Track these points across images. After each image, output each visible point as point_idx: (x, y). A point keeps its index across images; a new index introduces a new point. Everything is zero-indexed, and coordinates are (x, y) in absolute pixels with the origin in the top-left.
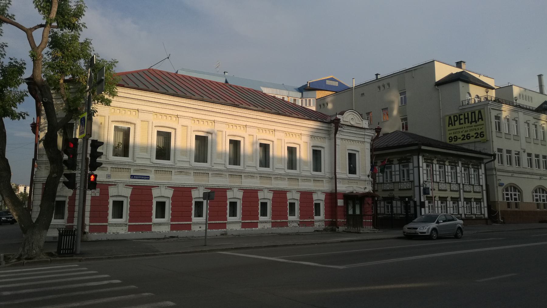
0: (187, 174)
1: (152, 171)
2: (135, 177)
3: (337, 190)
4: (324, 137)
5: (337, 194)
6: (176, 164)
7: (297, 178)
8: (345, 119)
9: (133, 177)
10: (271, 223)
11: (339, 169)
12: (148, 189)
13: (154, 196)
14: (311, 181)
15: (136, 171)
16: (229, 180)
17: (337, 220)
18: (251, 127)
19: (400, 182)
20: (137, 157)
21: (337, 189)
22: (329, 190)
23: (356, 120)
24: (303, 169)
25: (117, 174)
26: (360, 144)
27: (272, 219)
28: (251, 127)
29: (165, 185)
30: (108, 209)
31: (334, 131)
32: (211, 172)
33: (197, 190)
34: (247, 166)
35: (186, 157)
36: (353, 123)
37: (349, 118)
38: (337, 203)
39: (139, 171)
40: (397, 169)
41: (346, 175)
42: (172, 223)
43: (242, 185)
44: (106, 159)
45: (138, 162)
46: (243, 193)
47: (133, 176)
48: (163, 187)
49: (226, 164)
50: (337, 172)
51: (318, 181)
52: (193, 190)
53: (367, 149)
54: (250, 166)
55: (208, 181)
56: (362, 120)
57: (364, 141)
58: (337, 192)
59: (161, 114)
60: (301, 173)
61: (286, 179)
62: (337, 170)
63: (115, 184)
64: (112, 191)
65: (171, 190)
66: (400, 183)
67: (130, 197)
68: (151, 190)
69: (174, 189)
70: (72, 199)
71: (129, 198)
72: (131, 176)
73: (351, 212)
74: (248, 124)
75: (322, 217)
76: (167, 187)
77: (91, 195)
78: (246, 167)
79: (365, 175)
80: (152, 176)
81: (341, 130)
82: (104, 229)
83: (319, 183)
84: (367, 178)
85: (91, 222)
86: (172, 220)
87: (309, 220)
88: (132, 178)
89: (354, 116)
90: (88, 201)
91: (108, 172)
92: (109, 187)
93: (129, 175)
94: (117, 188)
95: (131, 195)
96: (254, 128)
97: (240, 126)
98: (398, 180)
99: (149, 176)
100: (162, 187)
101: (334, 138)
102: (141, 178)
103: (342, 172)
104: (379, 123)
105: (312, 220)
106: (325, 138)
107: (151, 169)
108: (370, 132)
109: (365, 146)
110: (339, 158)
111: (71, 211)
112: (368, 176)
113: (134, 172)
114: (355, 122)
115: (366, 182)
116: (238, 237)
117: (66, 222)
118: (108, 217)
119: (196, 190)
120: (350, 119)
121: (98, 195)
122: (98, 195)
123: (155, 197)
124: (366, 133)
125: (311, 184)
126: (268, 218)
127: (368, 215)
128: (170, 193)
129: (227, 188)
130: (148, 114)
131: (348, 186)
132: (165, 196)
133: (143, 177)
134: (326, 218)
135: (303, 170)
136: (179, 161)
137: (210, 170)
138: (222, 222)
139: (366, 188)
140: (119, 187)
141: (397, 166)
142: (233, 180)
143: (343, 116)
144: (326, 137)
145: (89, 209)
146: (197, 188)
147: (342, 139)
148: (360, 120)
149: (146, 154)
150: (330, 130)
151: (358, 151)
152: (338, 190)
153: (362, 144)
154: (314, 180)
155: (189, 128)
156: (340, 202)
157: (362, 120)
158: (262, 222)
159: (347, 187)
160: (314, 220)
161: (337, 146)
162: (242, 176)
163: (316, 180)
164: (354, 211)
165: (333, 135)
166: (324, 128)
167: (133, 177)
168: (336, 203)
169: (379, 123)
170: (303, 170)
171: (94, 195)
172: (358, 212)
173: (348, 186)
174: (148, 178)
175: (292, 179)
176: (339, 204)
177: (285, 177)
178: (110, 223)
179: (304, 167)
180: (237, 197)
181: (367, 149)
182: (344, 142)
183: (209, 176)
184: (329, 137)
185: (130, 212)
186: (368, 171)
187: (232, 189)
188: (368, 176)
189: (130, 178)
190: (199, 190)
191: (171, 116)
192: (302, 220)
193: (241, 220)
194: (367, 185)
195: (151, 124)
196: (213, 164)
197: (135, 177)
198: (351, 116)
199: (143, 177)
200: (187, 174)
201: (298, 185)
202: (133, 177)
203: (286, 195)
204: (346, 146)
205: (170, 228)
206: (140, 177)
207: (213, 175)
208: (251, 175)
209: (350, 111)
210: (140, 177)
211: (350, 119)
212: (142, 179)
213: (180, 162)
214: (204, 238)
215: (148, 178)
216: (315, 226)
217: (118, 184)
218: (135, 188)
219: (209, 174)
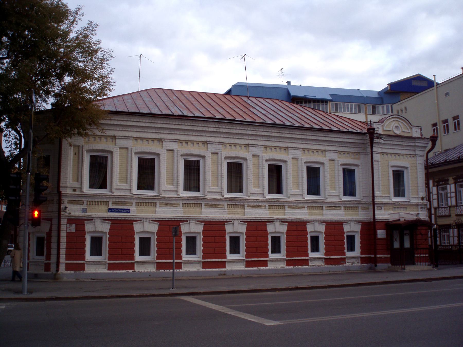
0: (174, 205)
2: (113, 210)
3: (376, 219)
4: (359, 152)
5: (376, 223)
6: (161, 194)
7: (321, 205)
8: (386, 127)
9: (111, 210)
10: (285, 261)
11: (379, 192)
12: (130, 223)
13: (135, 231)
14: (341, 208)
15: (113, 203)
16: (228, 210)
17: (375, 256)
18: (255, 146)
19: (457, 206)
20: (115, 188)
21: (376, 217)
22: (365, 219)
23: (401, 128)
24: (329, 194)
25: (94, 208)
26: (410, 158)
27: (287, 257)
28: (254, 145)
29: (149, 219)
30: (84, 246)
31: (369, 144)
32: (205, 203)
33: (188, 223)
34: (251, 193)
35: (172, 186)
36: (397, 132)
37: (392, 126)
38: (377, 234)
39: (119, 203)
40: (453, 189)
41: (390, 198)
42: (158, 261)
43: (245, 216)
44: (81, 192)
45: (116, 193)
46: (246, 226)
47: (112, 209)
48: (146, 221)
49: (223, 191)
50: (375, 195)
51: (350, 208)
52: (183, 224)
53: (421, 164)
54: (255, 194)
55: (201, 213)
56: (412, 127)
57: (415, 154)
58: (376, 221)
59: (142, 139)
60: (327, 199)
61: (306, 207)
62: (376, 193)
63: (90, 219)
64: (89, 227)
65: (156, 224)
66: (456, 207)
67: (109, 232)
68: (133, 224)
69: (159, 223)
70: (49, 234)
71: (107, 233)
72: (109, 209)
73: (396, 245)
74: (251, 142)
75: (357, 252)
76: (151, 220)
77: (66, 230)
78: (249, 194)
79: (418, 198)
80: (133, 208)
81: (380, 142)
82: (81, 267)
83: (352, 211)
84: (421, 201)
85: (67, 259)
86: (158, 258)
87: (339, 257)
89: (400, 123)
90: (64, 237)
91: (84, 206)
92: (85, 222)
93: (107, 208)
95: (110, 230)
96: (260, 146)
97: (240, 145)
98: (454, 203)
99: (129, 209)
100: (144, 221)
101: (370, 153)
102: (120, 212)
103: (384, 196)
105: (343, 257)
106: (359, 153)
107: (132, 201)
108: (423, 142)
109: (416, 160)
110: (379, 177)
111: (49, 248)
112: (423, 199)
114: (401, 130)
115: (419, 207)
116: (240, 277)
117: (45, 260)
118: (85, 254)
119: (186, 224)
120: (393, 127)
121: (73, 230)
122: (73, 230)
123: (137, 233)
124: (417, 144)
125: (341, 212)
126: (282, 255)
127: (421, 249)
128: (154, 228)
129: (226, 220)
130: (127, 140)
131: (392, 212)
132: (149, 231)
133: (122, 211)
134: (362, 253)
135: (328, 196)
136: (165, 191)
137: (202, 199)
138: (220, 260)
139: (418, 214)
140: (96, 222)
141: (453, 186)
142: (233, 211)
143: (382, 124)
144: (361, 151)
145: (65, 246)
146: (187, 221)
147: (383, 153)
148: (408, 128)
149: (125, 184)
150: (365, 142)
151: (406, 168)
152: (378, 219)
153: (413, 158)
154: (345, 207)
155: (176, 152)
156: (381, 234)
157: (412, 127)
158: (273, 260)
159: (392, 214)
160: (345, 257)
161: (374, 163)
162: (245, 205)
163: (348, 207)
164: (402, 243)
165: (369, 150)
166: (357, 141)
167: (111, 210)
168: (376, 234)
170: (328, 196)
171: (70, 231)
172: (407, 245)
173: (392, 212)
174: (128, 211)
175: (312, 206)
176: (379, 236)
177: (304, 205)
178: (87, 260)
179: (330, 191)
180: (238, 231)
181: (419, 164)
182: (386, 156)
183: (201, 207)
184: (365, 152)
185: (109, 248)
186: (422, 193)
187: (231, 221)
188: (423, 199)
191: (153, 140)
192: (328, 257)
193: (245, 258)
194: (420, 209)
195: (129, 151)
196: (206, 193)
197: (113, 210)
198: (394, 124)
199: (122, 211)
200: (175, 206)
201: (322, 214)
203: (306, 227)
204: (389, 162)
205: (156, 267)
206: (120, 210)
207: (207, 205)
208: (257, 204)
209: (393, 116)
211: (394, 127)
212: (122, 212)
213: (166, 192)
214: (172, 278)
215: (128, 211)
216: (348, 264)
217: (95, 218)
218: (115, 223)
219: (202, 205)
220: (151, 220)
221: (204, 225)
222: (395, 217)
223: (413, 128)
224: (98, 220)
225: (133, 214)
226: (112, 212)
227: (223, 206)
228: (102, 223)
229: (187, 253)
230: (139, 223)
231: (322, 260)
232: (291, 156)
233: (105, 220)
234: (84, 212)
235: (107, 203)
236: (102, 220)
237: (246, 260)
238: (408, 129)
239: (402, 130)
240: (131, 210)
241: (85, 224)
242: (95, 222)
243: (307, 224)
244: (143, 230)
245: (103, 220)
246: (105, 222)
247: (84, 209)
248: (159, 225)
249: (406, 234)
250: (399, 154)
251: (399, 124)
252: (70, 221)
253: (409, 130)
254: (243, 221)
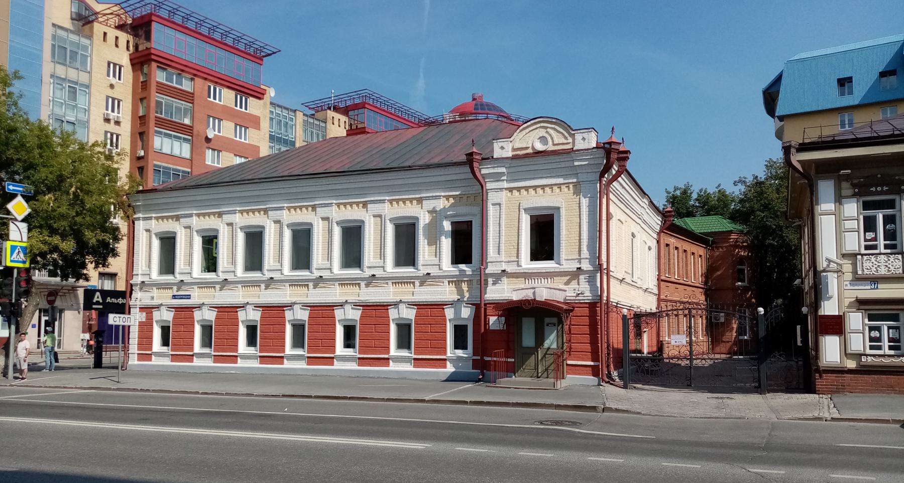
9: (174, 297)
12: (190, 309)
44: (150, 279)
56: (573, 132)
72: (173, 296)
89: (548, 130)
99: (190, 295)
102: (182, 298)
104: (613, 129)
121: (144, 320)
122: (144, 320)
133: (184, 297)
134: (474, 355)
143: (511, 139)
157: (573, 132)
169: (613, 129)
174: (188, 297)
190: (246, 310)
199: (184, 297)
206: (182, 297)
210: (182, 297)
215: (188, 297)
218: (178, 309)
220: (210, 307)
222: (527, 295)
223: (576, 134)
225: (263, 300)
230: (198, 310)
232: (371, 213)
233: (170, 307)
237: (413, 357)
238: (566, 138)
239: (553, 141)
240: (192, 297)
243: (389, 307)
249: (551, 324)
250: (543, 187)
251: (547, 132)
252: (142, 309)
253: (569, 138)
254: (305, 305)
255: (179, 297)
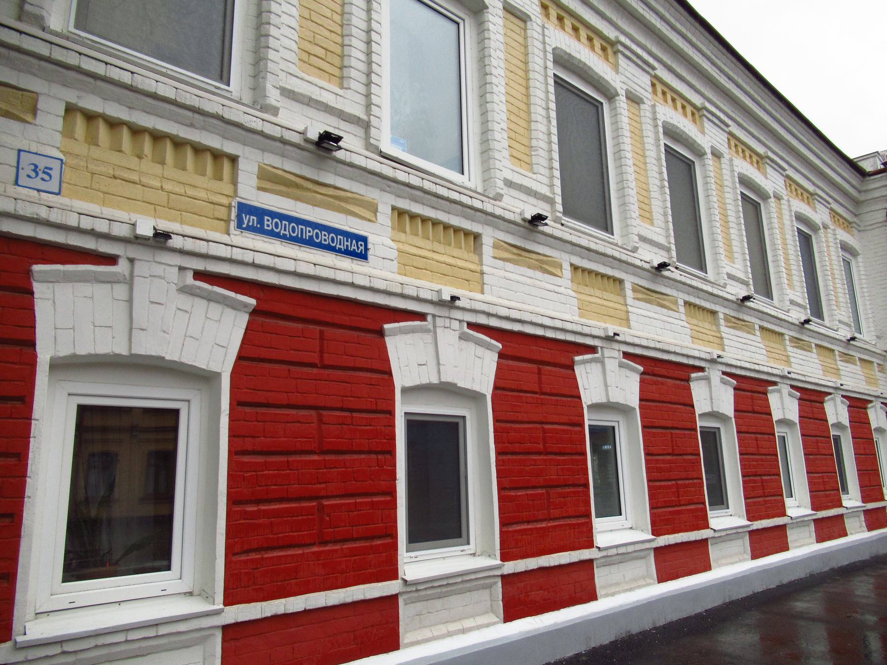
1: (381, 208)
39: (297, 186)
47: (260, 213)
65: (489, 347)
68: (381, 333)
72: (245, 209)
88: (250, 229)
94: (121, 291)
100: (439, 322)
102: (310, 243)
107: (371, 194)
113: (260, 189)
123: (405, 390)
133: (325, 238)
189: (233, 225)
202: (261, 221)
206: (309, 232)
221: (643, 373)
224: (158, 270)
226: (260, 230)
227: (671, 302)
228: (185, 301)
229: (710, 510)
231: (859, 516)
234: (37, 183)
235: (227, 166)
236: (189, 280)
241: (38, 288)
242: (131, 284)
244: (435, 380)
245: (199, 275)
246: (210, 298)
247: (42, 163)
248: (501, 355)
255: (285, 228)
